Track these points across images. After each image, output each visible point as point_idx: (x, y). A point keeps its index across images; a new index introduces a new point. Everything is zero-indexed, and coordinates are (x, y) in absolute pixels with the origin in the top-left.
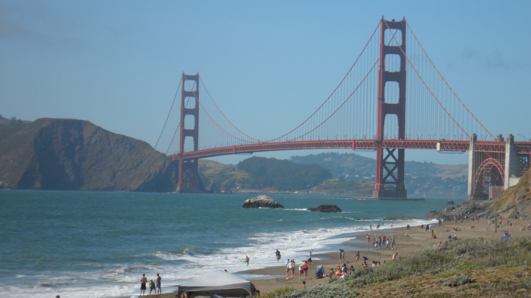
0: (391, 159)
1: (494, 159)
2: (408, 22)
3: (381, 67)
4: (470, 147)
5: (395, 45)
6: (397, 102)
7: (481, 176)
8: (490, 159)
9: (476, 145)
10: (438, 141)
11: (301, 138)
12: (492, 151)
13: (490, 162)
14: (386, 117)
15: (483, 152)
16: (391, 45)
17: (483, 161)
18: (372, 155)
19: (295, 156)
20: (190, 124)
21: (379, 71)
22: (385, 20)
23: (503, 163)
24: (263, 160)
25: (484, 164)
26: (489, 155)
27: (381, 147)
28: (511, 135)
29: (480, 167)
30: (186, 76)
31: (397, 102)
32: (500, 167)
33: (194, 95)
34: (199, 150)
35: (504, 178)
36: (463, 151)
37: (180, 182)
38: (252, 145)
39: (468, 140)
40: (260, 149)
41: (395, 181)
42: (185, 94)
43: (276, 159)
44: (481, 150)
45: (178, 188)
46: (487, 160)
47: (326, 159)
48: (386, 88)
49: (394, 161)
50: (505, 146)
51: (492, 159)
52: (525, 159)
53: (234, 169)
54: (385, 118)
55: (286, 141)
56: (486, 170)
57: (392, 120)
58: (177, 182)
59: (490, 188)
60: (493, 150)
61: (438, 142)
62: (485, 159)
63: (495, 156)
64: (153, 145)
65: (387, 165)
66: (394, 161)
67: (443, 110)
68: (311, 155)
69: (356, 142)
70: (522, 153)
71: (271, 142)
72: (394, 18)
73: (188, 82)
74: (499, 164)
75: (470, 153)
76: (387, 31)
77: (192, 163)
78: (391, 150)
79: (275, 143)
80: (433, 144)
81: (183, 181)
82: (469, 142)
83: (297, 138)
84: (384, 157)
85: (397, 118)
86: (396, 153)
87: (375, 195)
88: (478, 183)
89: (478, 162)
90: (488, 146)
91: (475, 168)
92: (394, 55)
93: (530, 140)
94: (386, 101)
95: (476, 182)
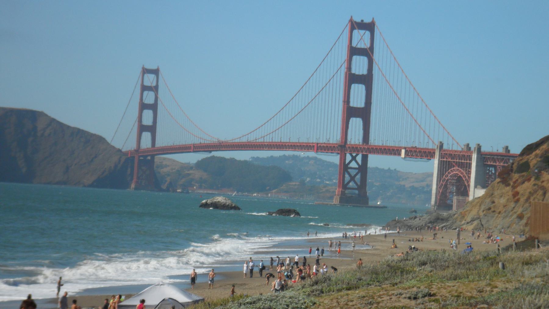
1: (460, 169)
2: (377, 24)
3: (347, 69)
4: (436, 155)
7: (446, 186)
8: (456, 168)
9: (442, 153)
10: (403, 148)
11: (263, 138)
12: (458, 161)
13: (456, 172)
15: (449, 161)
16: (359, 46)
18: (335, 159)
19: (255, 157)
21: (346, 72)
22: (354, 21)
23: (469, 173)
24: (222, 160)
25: (449, 173)
26: (455, 165)
27: (344, 151)
28: (479, 145)
29: (446, 176)
30: (146, 69)
32: (465, 177)
33: (154, 89)
34: (156, 146)
36: (428, 159)
37: (135, 179)
38: (211, 143)
39: (434, 148)
40: (220, 148)
42: (144, 88)
45: (133, 186)
46: (452, 169)
47: (287, 162)
49: (357, 166)
50: (472, 155)
51: (457, 168)
52: (492, 170)
53: (191, 168)
55: (246, 141)
56: (452, 180)
57: (356, 123)
58: (132, 179)
59: (455, 199)
61: (403, 149)
62: (451, 168)
63: (461, 165)
64: (109, 140)
65: (349, 170)
66: (357, 166)
68: (272, 156)
69: (319, 145)
70: (489, 163)
71: (231, 141)
72: (362, 19)
73: (148, 76)
74: (465, 174)
75: (436, 162)
76: (355, 32)
77: (148, 160)
78: (354, 155)
79: (235, 143)
80: (398, 150)
82: (434, 150)
83: (259, 139)
84: (347, 161)
86: (359, 158)
87: (336, 201)
88: (442, 192)
90: (455, 155)
91: (440, 178)
92: (362, 57)
94: (352, 104)
95: (441, 191)
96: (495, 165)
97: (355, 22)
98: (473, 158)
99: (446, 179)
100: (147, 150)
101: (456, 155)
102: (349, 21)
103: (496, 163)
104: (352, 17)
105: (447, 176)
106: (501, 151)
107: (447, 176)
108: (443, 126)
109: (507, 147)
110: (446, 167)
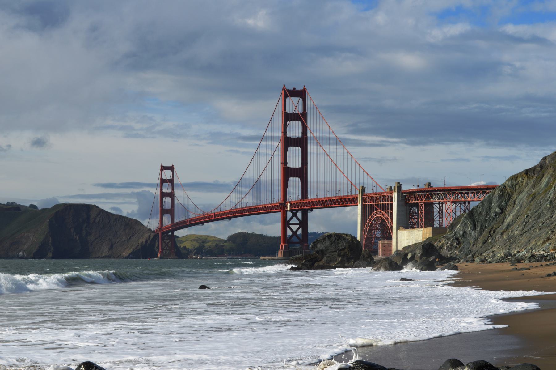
0: (294, 220)
1: (382, 211)
2: (307, 91)
4: (359, 202)
5: (297, 112)
6: (300, 166)
7: (370, 231)
9: (364, 197)
12: (379, 203)
14: (289, 180)
15: (371, 204)
16: (295, 113)
17: (371, 214)
27: (285, 209)
28: (399, 183)
29: (369, 221)
30: (163, 167)
31: (300, 166)
37: (160, 251)
41: (299, 241)
42: (163, 181)
44: (369, 202)
45: (159, 255)
46: (375, 212)
48: (288, 154)
51: (379, 211)
53: (225, 241)
57: (295, 182)
59: (380, 243)
60: (380, 202)
65: (291, 226)
67: (338, 169)
70: (411, 202)
71: (211, 213)
76: (288, 99)
77: (169, 235)
78: (295, 212)
81: (163, 249)
82: (358, 195)
84: (288, 219)
85: (300, 180)
86: (299, 215)
89: (366, 216)
92: (297, 122)
93: (418, 186)
95: (365, 237)
96: (417, 203)
97: (288, 90)
98: (394, 198)
99: (370, 223)
102: (282, 90)
104: (284, 86)
106: (422, 186)
108: (367, 173)
109: (429, 184)
110: (369, 211)
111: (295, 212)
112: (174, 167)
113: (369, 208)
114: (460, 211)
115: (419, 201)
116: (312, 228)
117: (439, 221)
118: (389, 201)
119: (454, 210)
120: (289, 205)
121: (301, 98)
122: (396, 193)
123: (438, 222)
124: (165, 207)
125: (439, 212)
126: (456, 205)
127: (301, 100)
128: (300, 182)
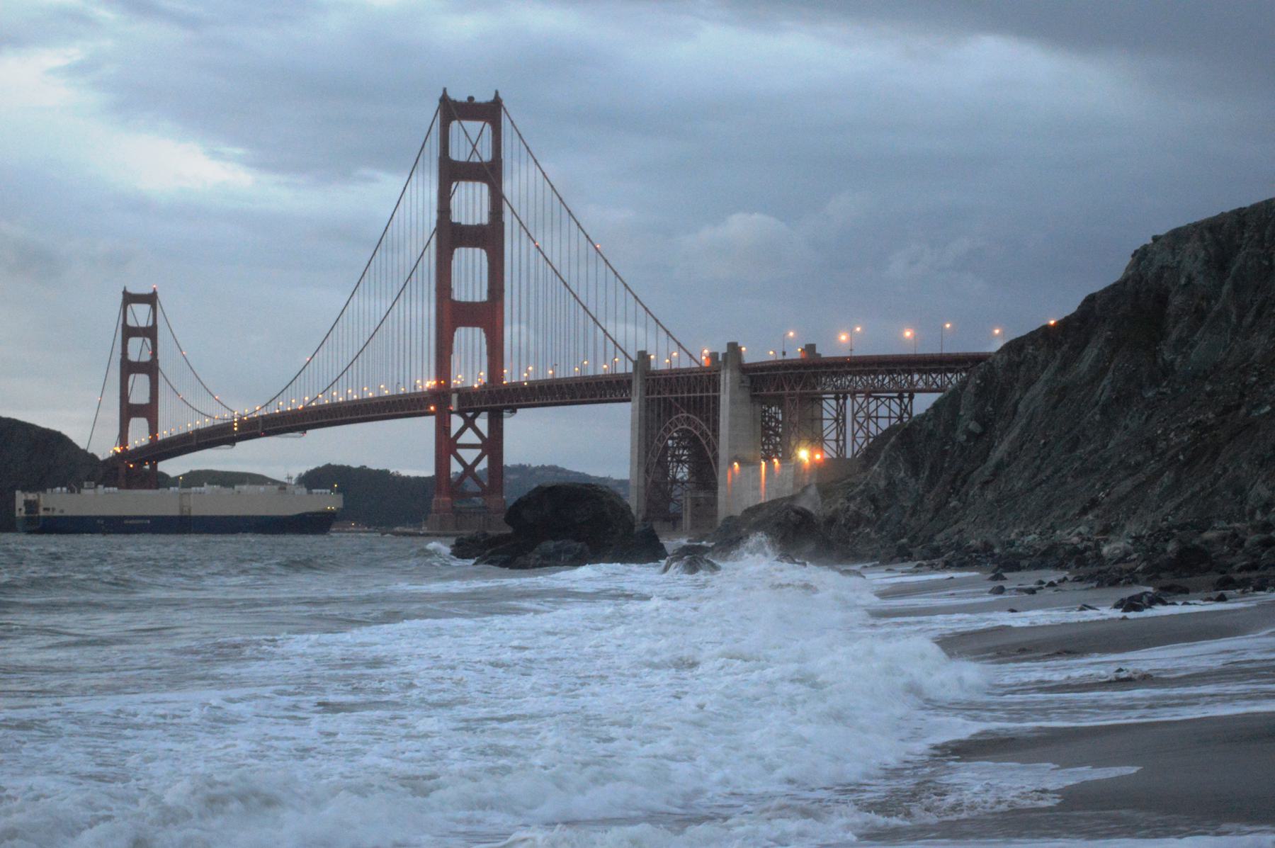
0: (469, 437)
1: (691, 416)
2: (505, 103)
5: (477, 160)
6: (485, 298)
12: (685, 395)
13: (682, 425)
14: (456, 334)
15: (665, 399)
16: (471, 160)
20: (139, 391)
23: (716, 423)
26: (678, 406)
29: (659, 440)
31: (485, 298)
32: (708, 436)
35: (717, 466)
38: (224, 424)
43: (369, 470)
44: (659, 393)
49: (478, 441)
51: (685, 415)
54: (453, 335)
60: (689, 392)
65: (460, 451)
66: (476, 440)
67: (581, 308)
70: (765, 392)
72: (471, 95)
74: (705, 427)
84: (453, 432)
85: (483, 335)
86: (482, 423)
91: (647, 445)
92: (478, 184)
93: (784, 354)
95: (650, 480)
98: (722, 383)
100: (139, 451)
101: (680, 379)
103: (784, 390)
105: (661, 438)
107: (661, 438)
111: (469, 414)
112: (159, 295)
113: (659, 405)
114: (890, 417)
115: (787, 391)
116: (511, 456)
117: (837, 441)
118: (711, 391)
119: (874, 414)
120: (455, 397)
121: (487, 125)
122: (728, 371)
123: (833, 445)
124: (134, 399)
125: (836, 420)
126: (879, 403)
127: (488, 128)
128: (484, 340)
